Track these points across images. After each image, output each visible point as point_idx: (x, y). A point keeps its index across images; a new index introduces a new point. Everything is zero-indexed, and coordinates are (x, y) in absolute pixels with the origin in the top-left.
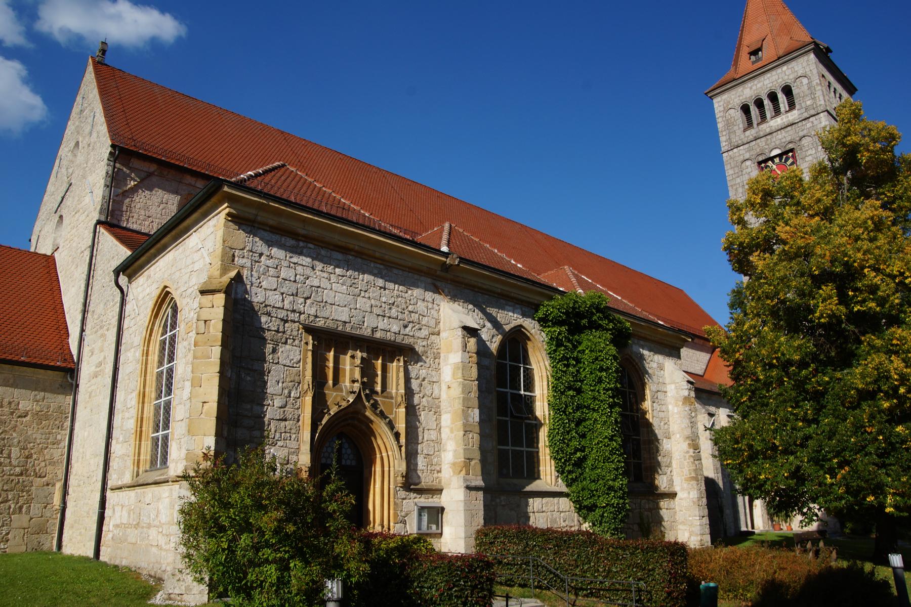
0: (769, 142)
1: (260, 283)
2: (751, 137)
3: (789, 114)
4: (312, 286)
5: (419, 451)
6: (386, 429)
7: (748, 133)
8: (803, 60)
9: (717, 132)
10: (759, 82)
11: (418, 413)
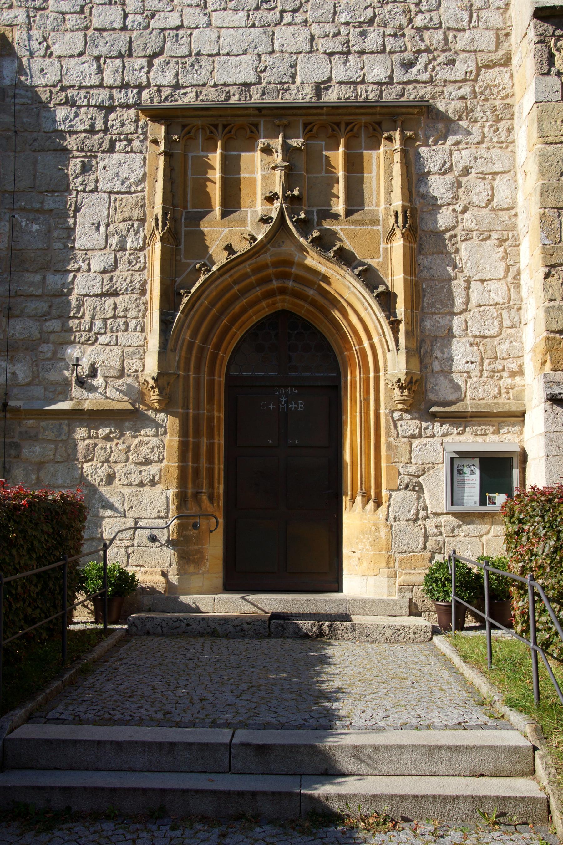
1: (48, 47)
4: (165, 29)
5: (456, 330)
11: (449, 248)
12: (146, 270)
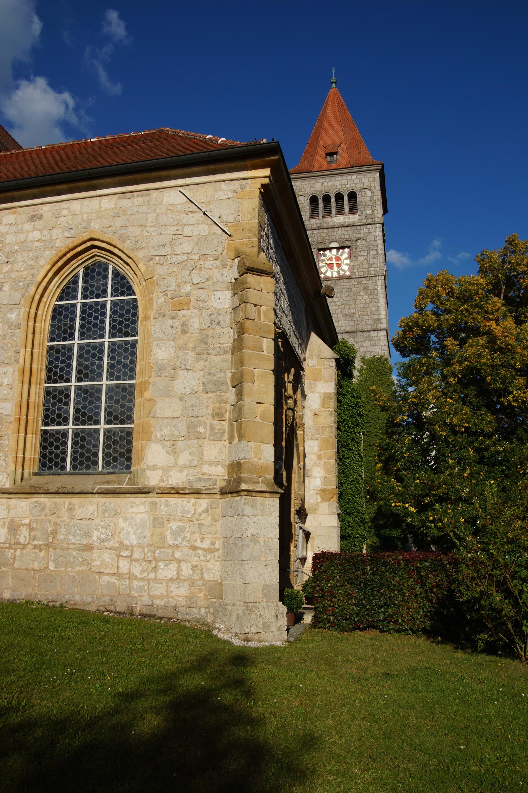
0: (330, 234)
2: (315, 225)
3: (351, 216)
7: (313, 221)
10: (330, 181)
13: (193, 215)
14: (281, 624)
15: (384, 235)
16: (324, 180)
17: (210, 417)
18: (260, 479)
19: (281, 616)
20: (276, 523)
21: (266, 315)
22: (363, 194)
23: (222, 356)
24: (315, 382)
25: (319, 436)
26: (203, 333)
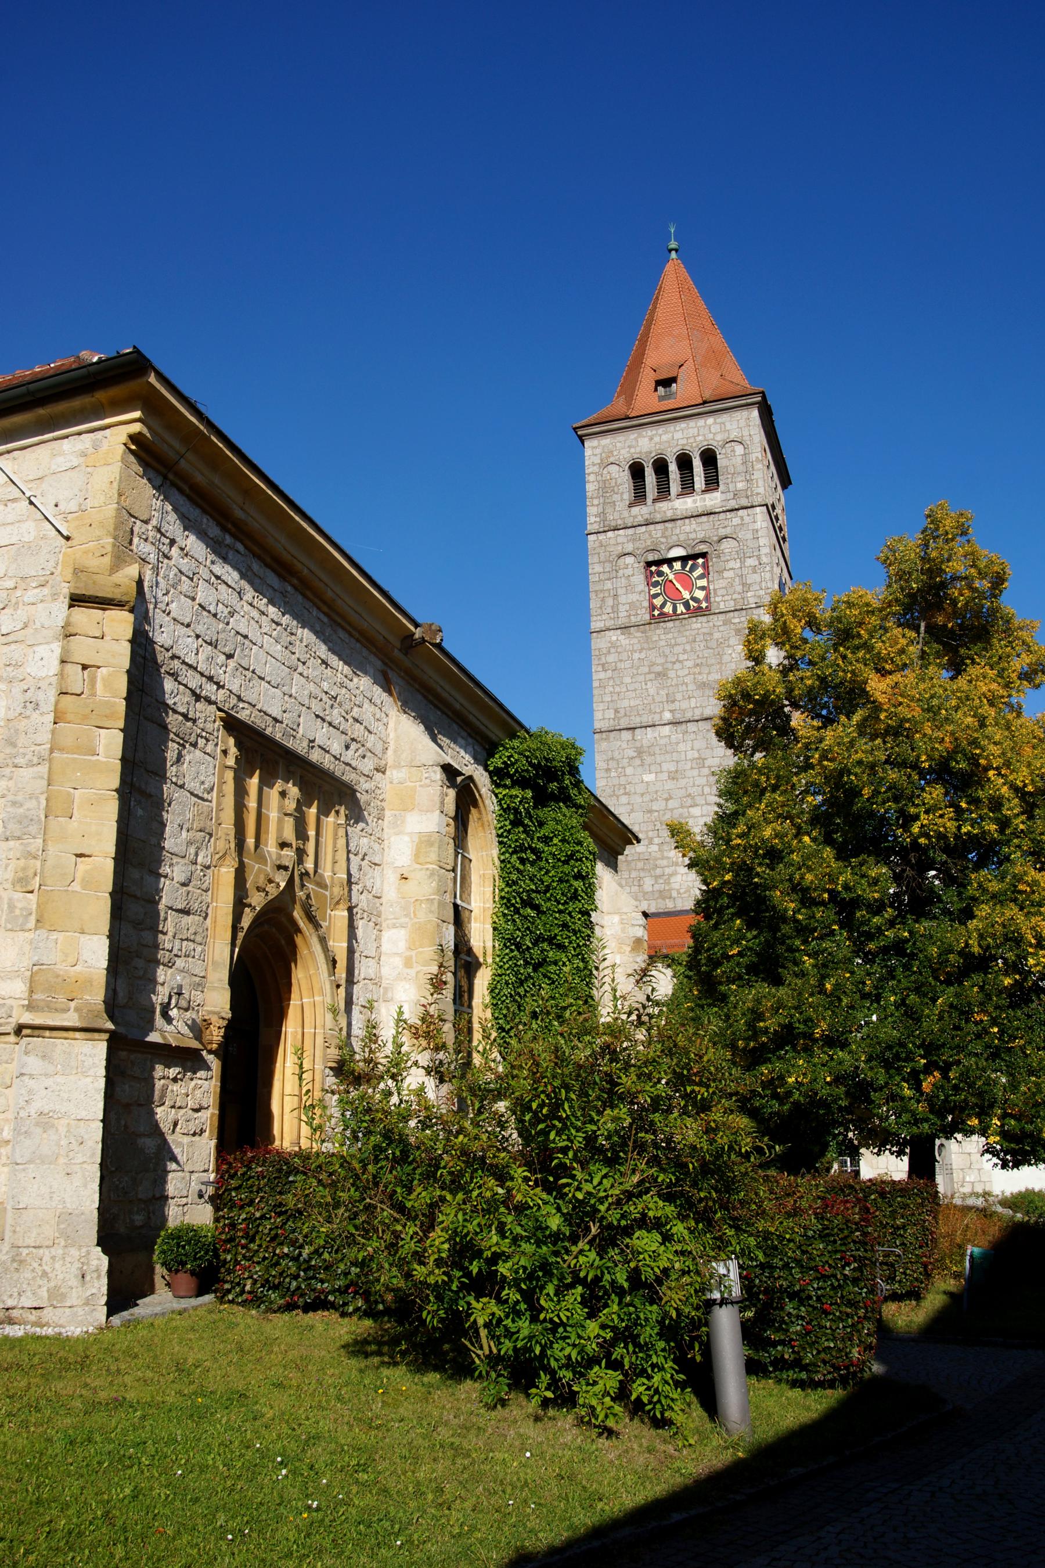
2: (640, 518)
3: (707, 496)
4: (238, 633)
6: (317, 948)
7: (635, 510)
8: (741, 415)
9: (585, 497)
10: (666, 433)
12: (210, 892)
13: (15, 504)
14: (94, 1291)
15: (777, 530)
16: (654, 432)
17: (8, 886)
18: (73, 1004)
19: (95, 1275)
20: (96, 1090)
21: (107, 683)
22: (729, 451)
23: (35, 769)
24: (403, 813)
25: (407, 920)
26: (10, 725)
